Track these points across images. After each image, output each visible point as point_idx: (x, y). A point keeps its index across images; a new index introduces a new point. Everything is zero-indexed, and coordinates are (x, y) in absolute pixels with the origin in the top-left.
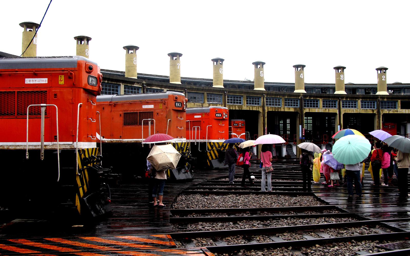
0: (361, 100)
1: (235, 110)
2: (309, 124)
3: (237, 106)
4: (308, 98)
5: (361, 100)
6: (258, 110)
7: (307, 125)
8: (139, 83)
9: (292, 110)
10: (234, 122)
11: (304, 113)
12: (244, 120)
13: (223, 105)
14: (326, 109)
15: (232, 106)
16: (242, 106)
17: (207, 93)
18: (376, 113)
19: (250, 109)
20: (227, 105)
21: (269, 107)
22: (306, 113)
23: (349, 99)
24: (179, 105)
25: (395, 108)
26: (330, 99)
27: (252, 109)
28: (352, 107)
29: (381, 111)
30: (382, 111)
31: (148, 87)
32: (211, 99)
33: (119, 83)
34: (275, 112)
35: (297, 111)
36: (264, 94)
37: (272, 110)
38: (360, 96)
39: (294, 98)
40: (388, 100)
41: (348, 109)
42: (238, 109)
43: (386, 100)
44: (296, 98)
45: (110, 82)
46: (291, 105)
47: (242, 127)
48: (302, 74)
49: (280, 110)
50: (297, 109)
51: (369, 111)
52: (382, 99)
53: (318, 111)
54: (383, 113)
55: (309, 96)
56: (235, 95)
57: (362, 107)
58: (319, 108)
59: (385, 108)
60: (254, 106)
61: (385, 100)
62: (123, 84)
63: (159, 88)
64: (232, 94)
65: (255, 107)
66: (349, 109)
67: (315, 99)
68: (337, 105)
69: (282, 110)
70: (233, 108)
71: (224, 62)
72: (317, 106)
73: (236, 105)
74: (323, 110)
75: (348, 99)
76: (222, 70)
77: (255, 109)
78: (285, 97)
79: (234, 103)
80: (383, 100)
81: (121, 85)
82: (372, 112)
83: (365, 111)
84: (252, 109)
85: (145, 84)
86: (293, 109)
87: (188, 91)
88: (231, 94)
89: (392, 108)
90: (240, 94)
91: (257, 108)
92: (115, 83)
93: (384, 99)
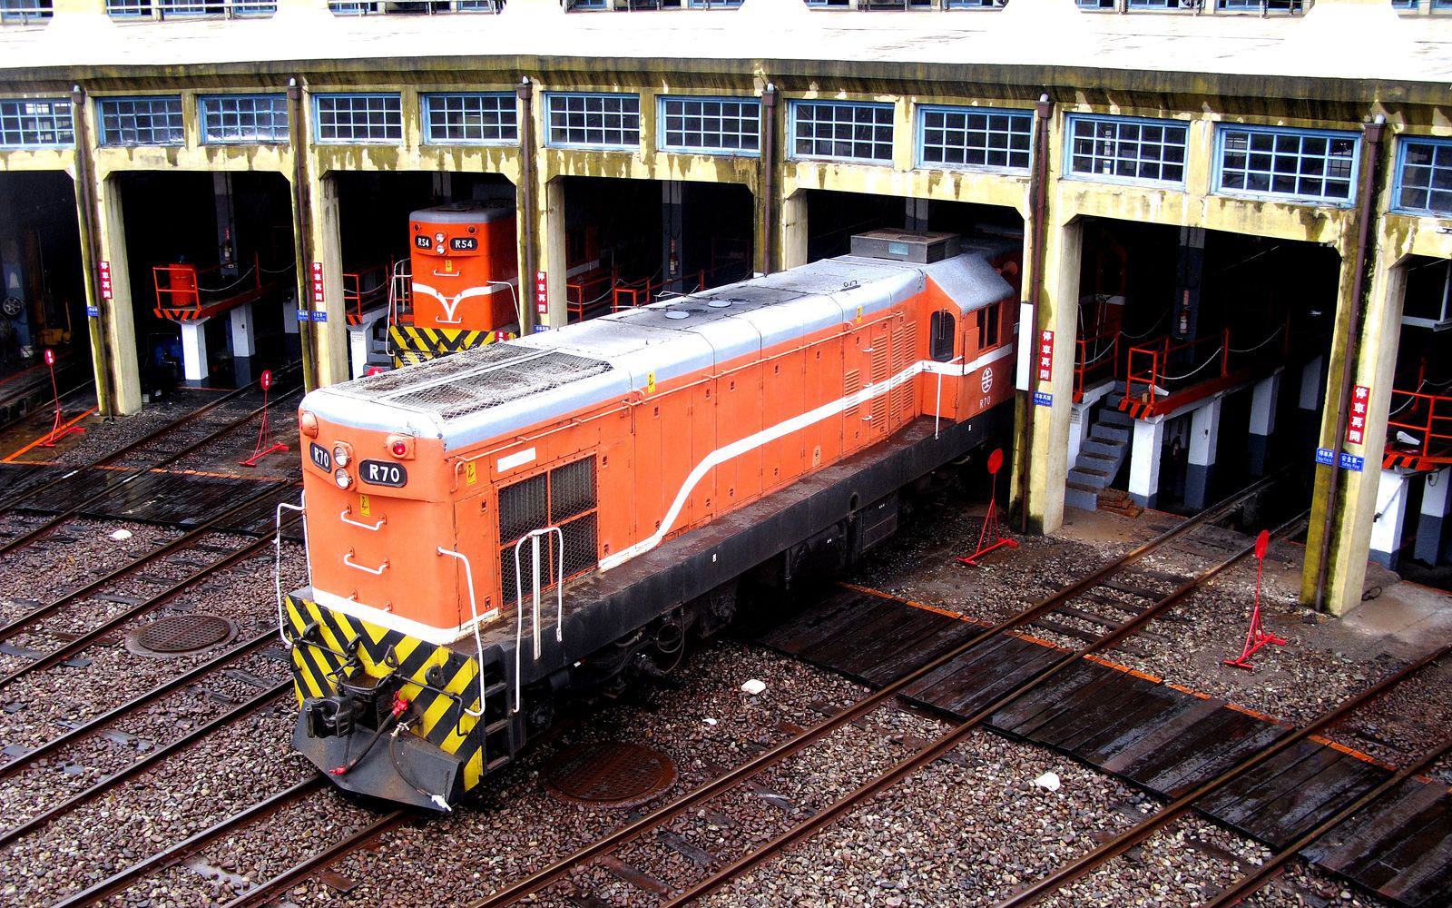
0: (1217, 117)
3: (365, 153)
5: (1217, 117)
6: (491, 169)
9: (704, 171)
13: (290, 149)
14: (934, 180)
15: (340, 150)
16: (393, 148)
17: (197, 96)
19: (441, 164)
20: (313, 147)
21: (561, 154)
23: (1121, 104)
26: (975, 103)
27: (458, 163)
28: (1150, 171)
29: (1388, 232)
30: (1395, 236)
32: (230, 120)
34: (595, 182)
35: (738, 179)
36: (528, 73)
37: (576, 169)
38: (1201, 88)
41: (1105, 189)
42: (375, 168)
49: (624, 169)
50: (739, 168)
51: (1277, 218)
52: (1408, 121)
54: (1398, 248)
57: (1230, 181)
60: (470, 151)
65: (477, 158)
66: (1116, 190)
69: (639, 172)
70: (343, 165)
73: (361, 148)
74: (918, 187)
75: (1114, 109)
77: (472, 165)
78: (657, 91)
79: (361, 132)
80: (1418, 129)
82: (1298, 233)
83: (1244, 219)
84: (458, 163)
90: (381, 86)
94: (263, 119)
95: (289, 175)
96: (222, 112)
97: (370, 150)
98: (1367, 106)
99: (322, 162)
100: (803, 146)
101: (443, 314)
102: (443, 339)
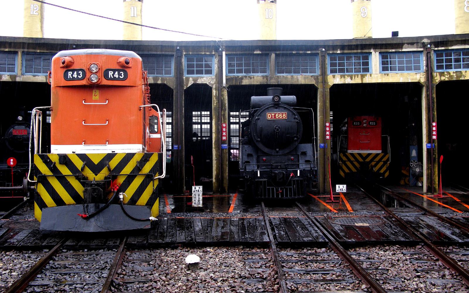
8: (415, 43)
24: (78, 74)
31: (440, 48)
33: (367, 51)
45: (346, 51)
62: (377, 50)
81: (371, 53)
85: (430, 44)
92: (359, 51)
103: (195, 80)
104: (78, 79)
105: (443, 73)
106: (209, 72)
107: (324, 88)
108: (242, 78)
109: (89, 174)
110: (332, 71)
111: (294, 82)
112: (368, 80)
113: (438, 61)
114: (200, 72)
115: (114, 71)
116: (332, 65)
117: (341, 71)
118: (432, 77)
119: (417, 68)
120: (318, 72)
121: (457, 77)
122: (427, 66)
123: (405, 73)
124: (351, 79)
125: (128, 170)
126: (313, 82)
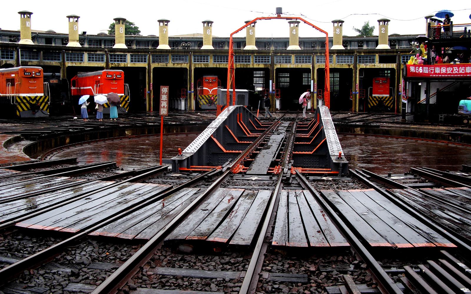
1: (201, 68)
2: (336, 78)
4: (279, 55)
7: (334, 79)
10: (205, 78)
11: (275, 69)
12: (216, 76)
13: (189, 64)
18: (353, 68)
19: (216, 66)
22: (277, 69)
25: (373, 62)
32: (177, 59)
33: (82, 52)
34: (244, 68)
35: (267, 67)
38: (335, 51)
39: (264, 55)
40: (365, 54)
43: (363, 54)
44: (266, 55)
45: (73, 52)
46: (262, 62)
47: (213, 82)
48: (294, 30)
53: (289, 66)
55: (280, 52)
56: (201, 55)
58: (291, 64)
59: (363, 63)
60: (221, 64)
61: (363, 54)
63: (122, 53)
64: (198, 54)
67: (286, 55)
68: (311, 61)
71: (213, 24)
72: (290, 62)
73: (202, 64)
74: (295, 66)
76: (209, 31)
77: (222, 66)
78: (254, 55)
79: (201, 61)
80: (360, 54)
82: (348, 67)
85: (108, 51)
86: (263, 66)
87: (153, 54)
88: (197, 54)
89: (370, 62)
91: (224, 65)
92: (79, 52)
93: (361, 54)
94: (183, 59)
95: (188, 68)
96: (175, 58)
97: (204, 64)
98: (355, 52)
99: (194, 66)
100: (277, 62)
101: (210, 93)
102: (209, 97)
103: (6, 61)
104: (28, 75)
105: (113, 63)
106: (12, 58)
107: (64, 67)
108: (28, 62)
109: (31, 102)
110: (68, 60)
111: (51, 64)
112: (82, 65)
113: (111, 58)
114: (8, 58)
115: (38, 73)
116: (67, 57)
117: (71, 60)
118: (108, 65)
119: (103, 61)
120: (61, 61)
121: (118, 65)
122: (106, 60)
123: (98, 62)
124: (76, 64)
125: (41, 101)
126: (59, 65)
